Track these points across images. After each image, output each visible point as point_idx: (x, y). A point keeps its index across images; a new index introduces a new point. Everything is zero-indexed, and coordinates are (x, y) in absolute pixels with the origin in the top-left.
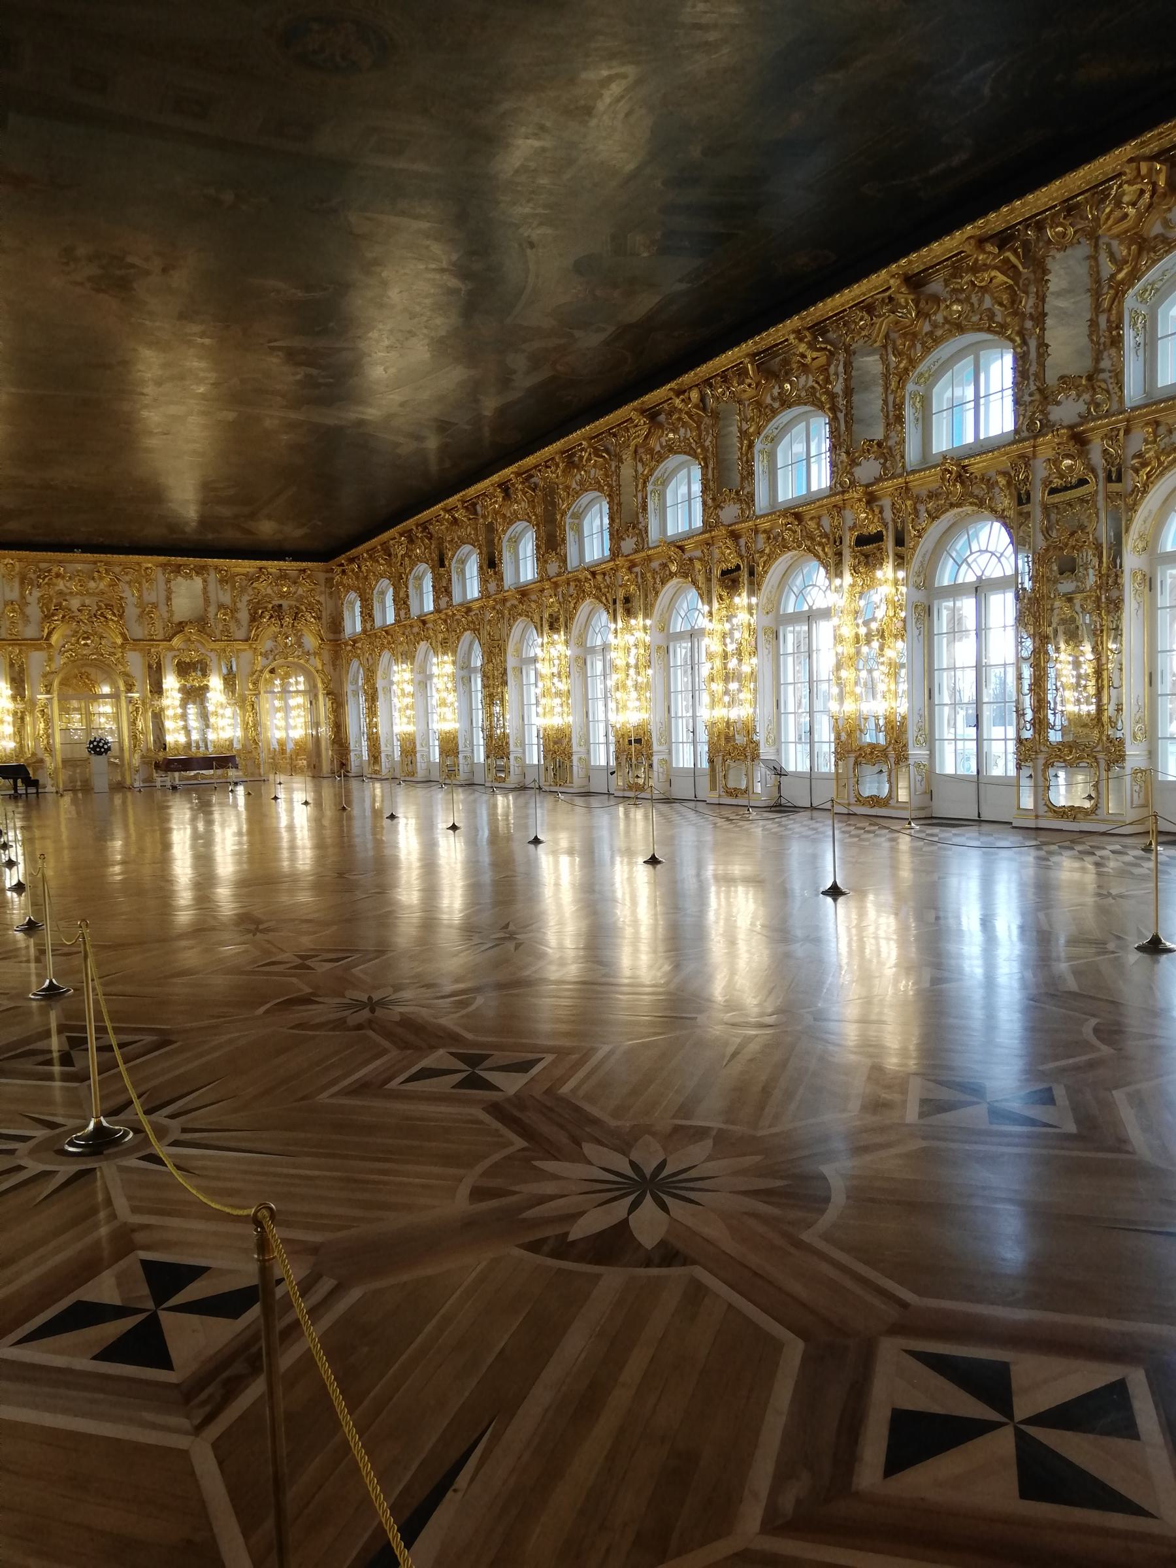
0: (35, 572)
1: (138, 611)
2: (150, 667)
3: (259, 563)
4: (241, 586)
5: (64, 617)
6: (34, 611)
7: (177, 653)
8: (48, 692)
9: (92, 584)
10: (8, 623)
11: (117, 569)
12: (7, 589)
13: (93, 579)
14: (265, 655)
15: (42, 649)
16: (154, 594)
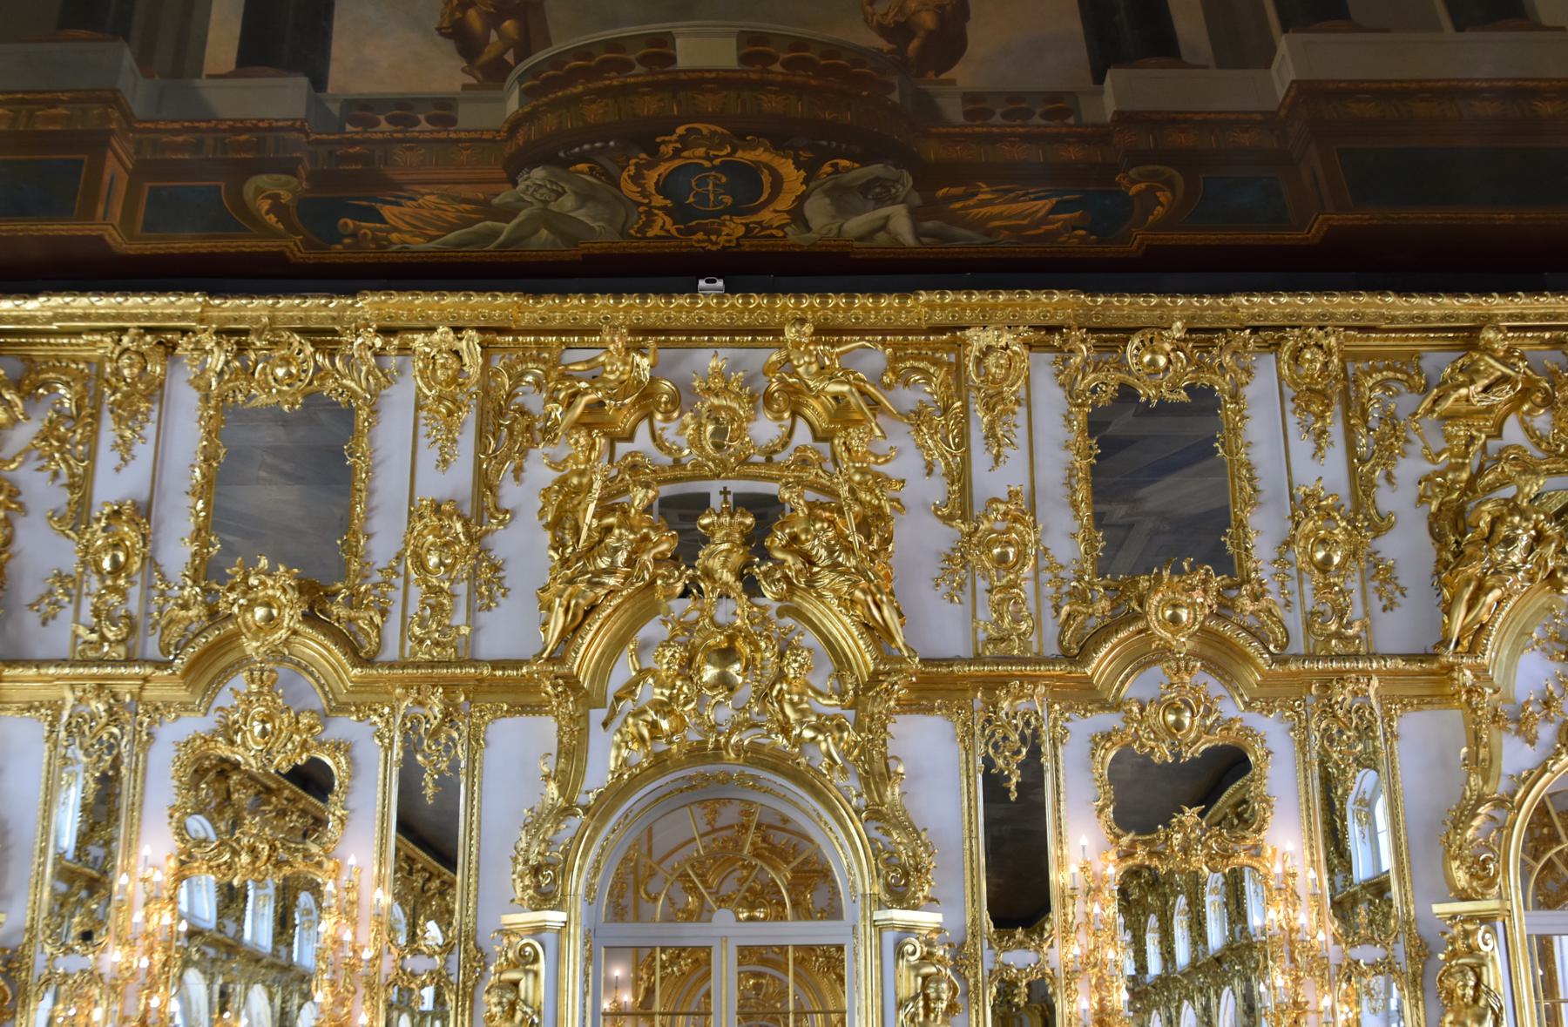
0: (538, 385)
1: (942, 537)
2: (994, 785)
3: (1462, 306)
4: (1390, 419)
5: (630, 562)
6: (524, 546)
7: (1110, 720)
8: (544, 899)
9: (765, 429)
10: (416, 593)
11: (874, 357)
12: (429, 456)
13: (768, 399)
14: (1520, 723)
15: (537, 709)
16: (1016, 458)
